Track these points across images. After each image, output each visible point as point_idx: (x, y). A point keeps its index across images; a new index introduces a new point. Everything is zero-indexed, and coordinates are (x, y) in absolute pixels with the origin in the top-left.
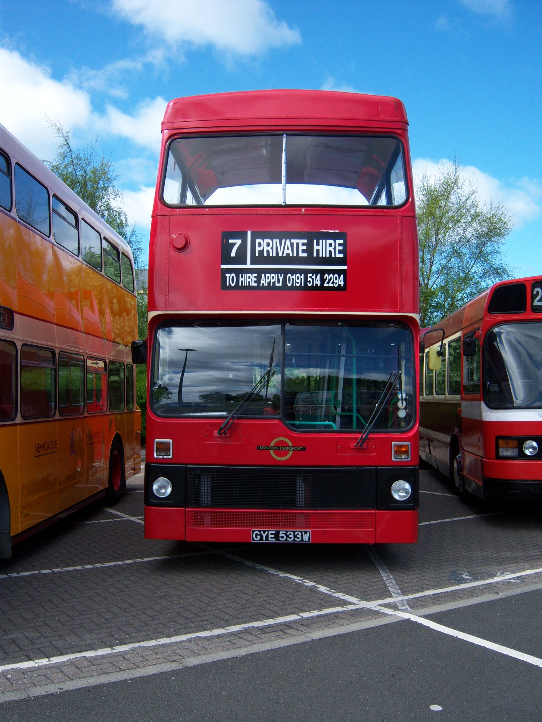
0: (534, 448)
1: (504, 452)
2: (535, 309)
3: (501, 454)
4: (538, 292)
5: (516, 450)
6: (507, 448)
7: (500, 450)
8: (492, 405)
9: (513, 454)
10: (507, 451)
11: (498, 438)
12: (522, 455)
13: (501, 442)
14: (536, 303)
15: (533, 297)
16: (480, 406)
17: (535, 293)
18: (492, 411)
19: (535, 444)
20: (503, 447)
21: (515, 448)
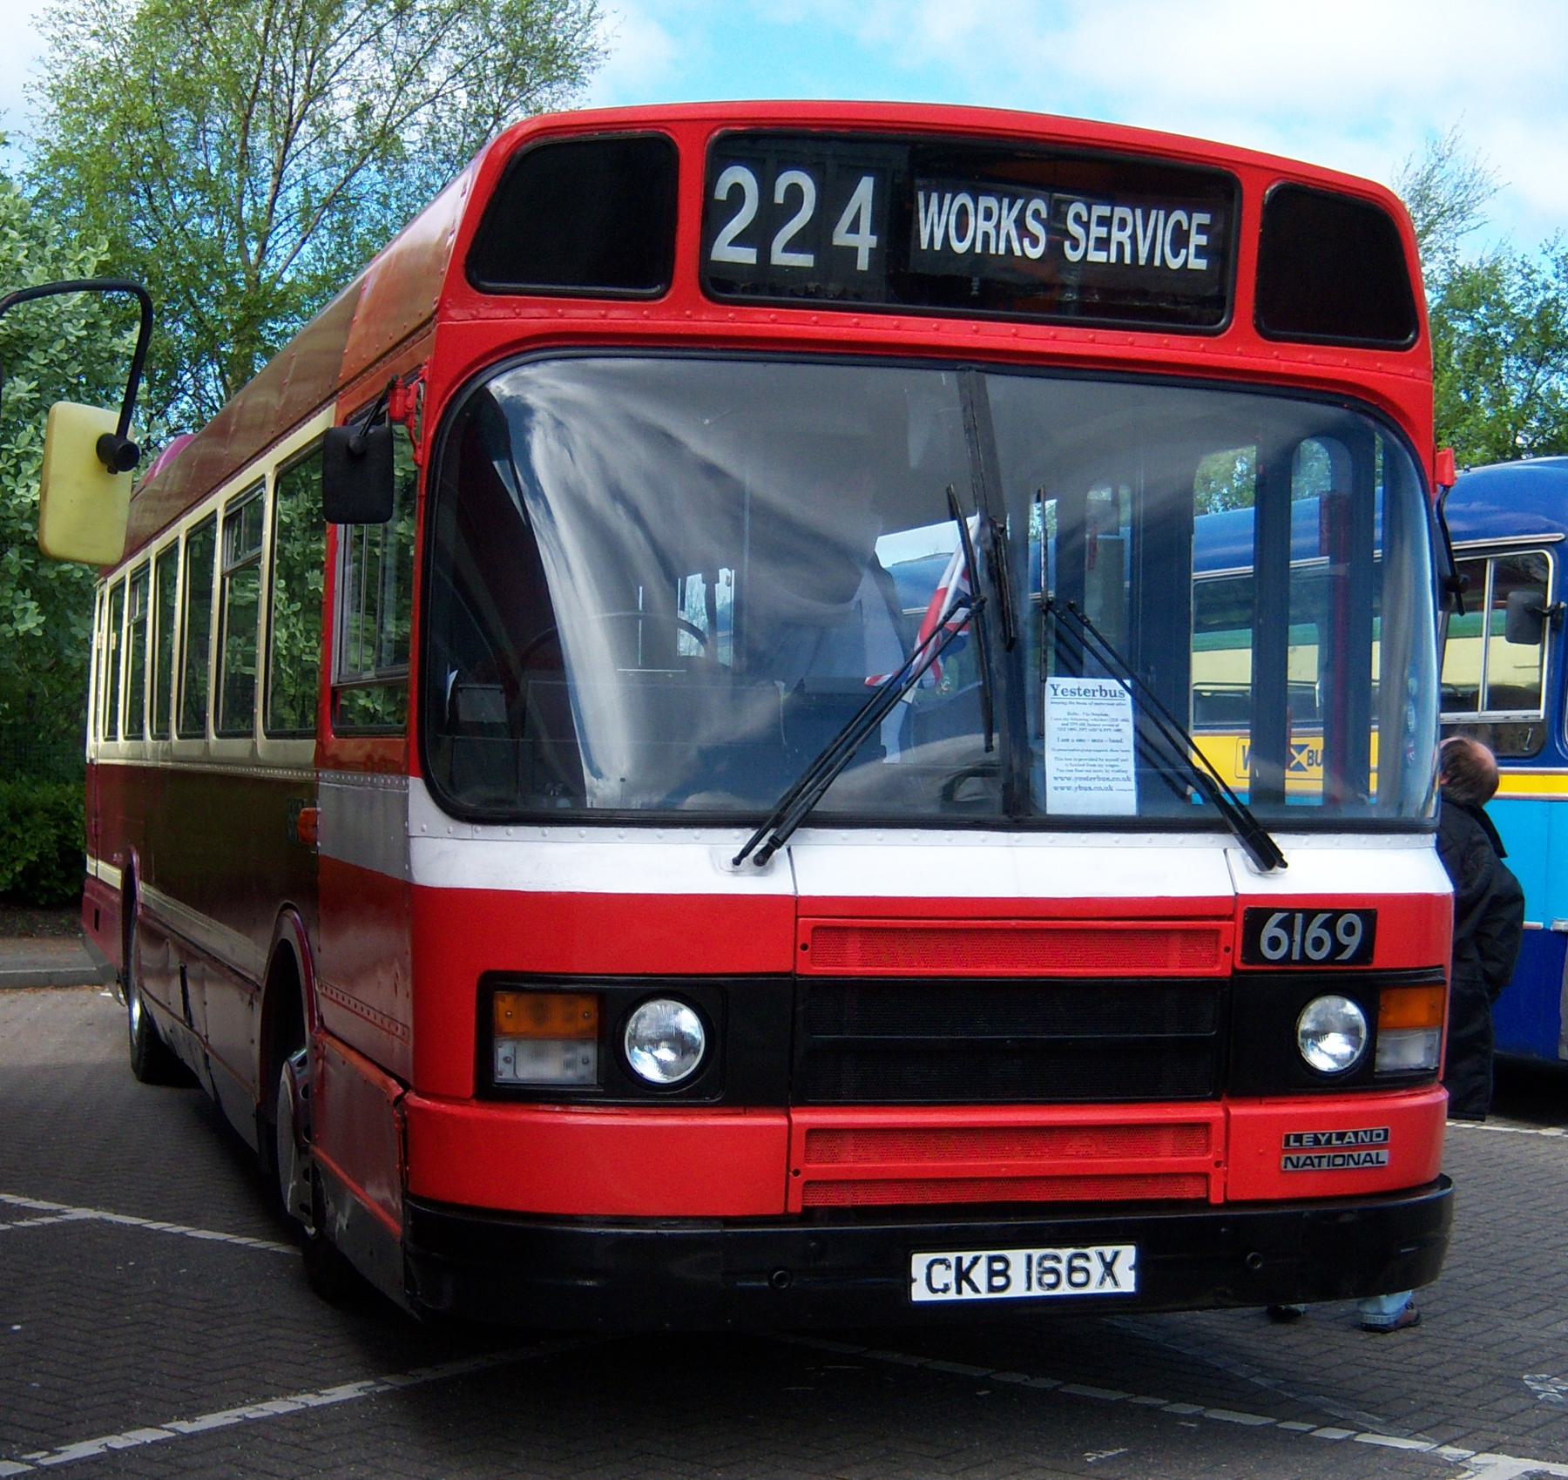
0: (680, 1042)
1: (524, 1064)
2: (720, 284)
3: (504, 1073)
4: (737, 191)
5: (589, 1052)
6: (538, 1038)
7: (503, 1050)
8: (464, 801)
9: (570, 1075)
10: (538, 1055)
11: (492, 984)
12: (620, 1084)
13: (506, 1006)
14: (725, 251)
15: (715, 215)
16: (405, 798)
17: (721, 193)
18: (467, 830)
19: (688, 1021)
20: (517, 1037)
21: (582, 1038)
